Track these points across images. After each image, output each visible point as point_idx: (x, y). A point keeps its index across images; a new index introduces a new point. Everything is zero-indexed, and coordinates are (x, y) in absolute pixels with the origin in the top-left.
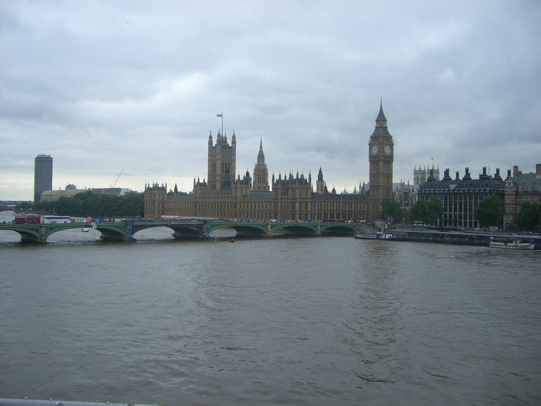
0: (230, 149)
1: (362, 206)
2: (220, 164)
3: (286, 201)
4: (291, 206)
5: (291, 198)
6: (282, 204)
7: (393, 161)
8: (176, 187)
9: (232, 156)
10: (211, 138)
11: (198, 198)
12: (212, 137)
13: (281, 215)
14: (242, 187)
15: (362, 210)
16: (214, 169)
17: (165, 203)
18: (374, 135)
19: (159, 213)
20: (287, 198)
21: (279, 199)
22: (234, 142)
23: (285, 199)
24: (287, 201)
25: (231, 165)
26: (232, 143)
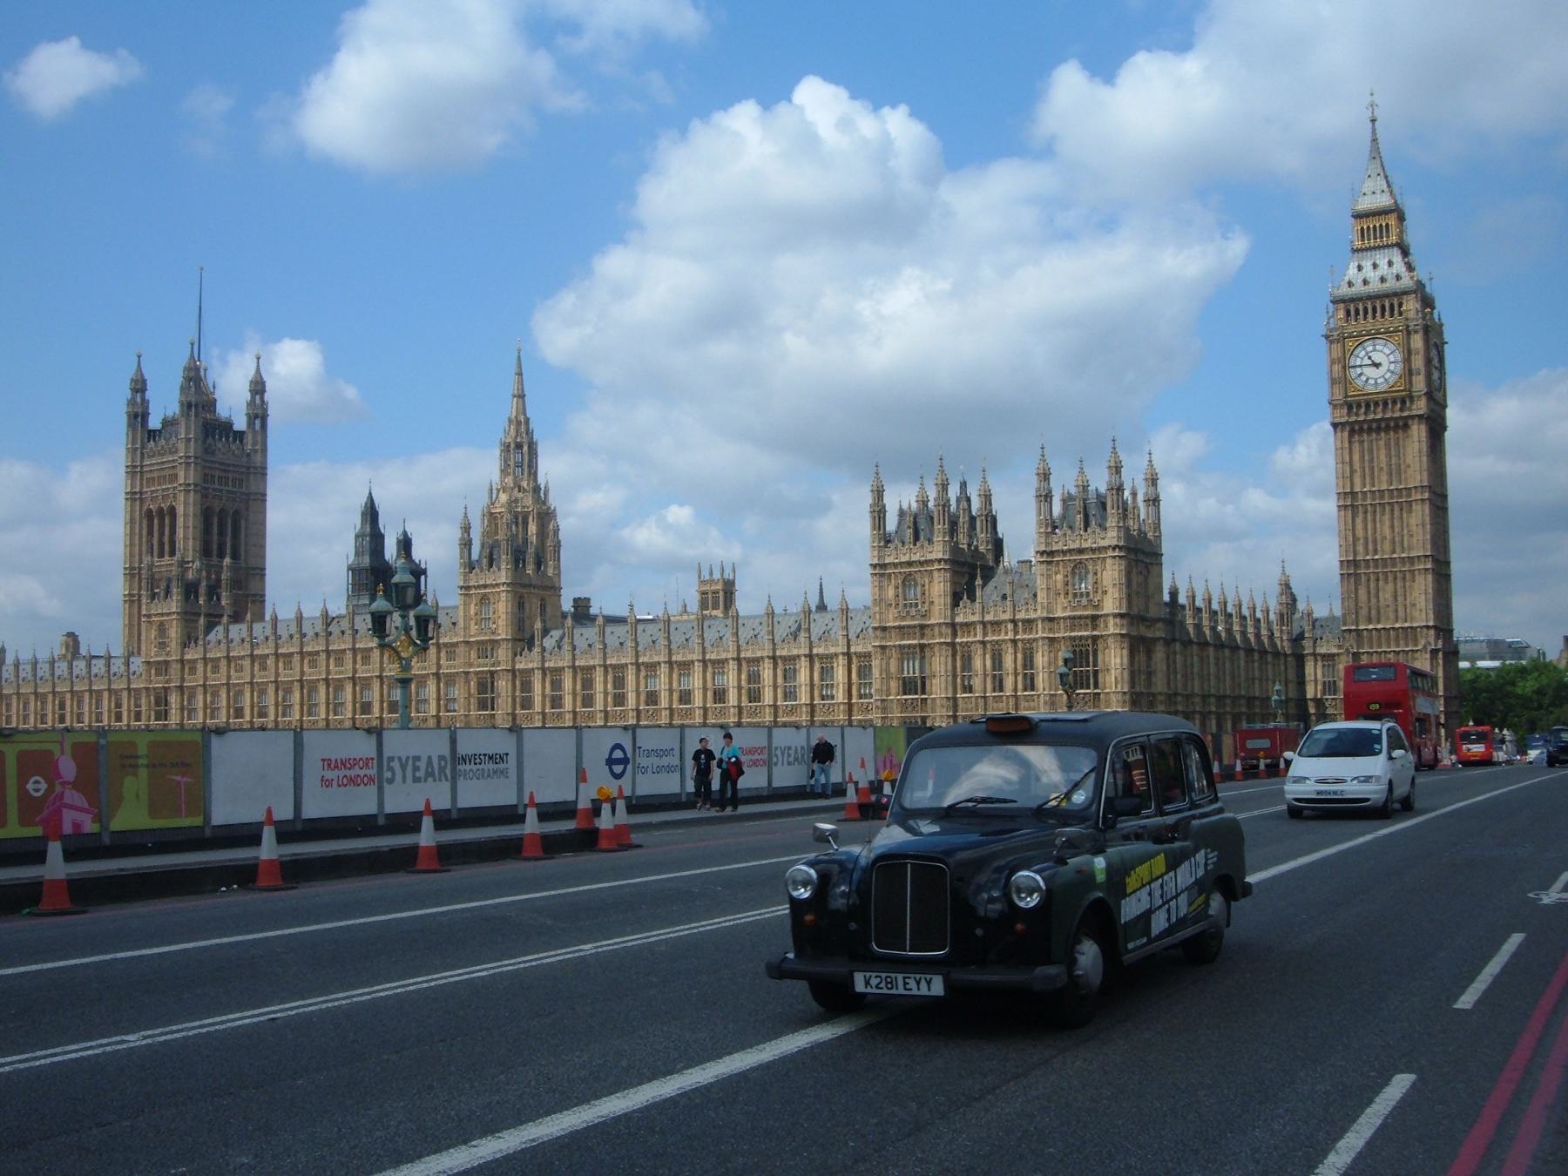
0: (241, 441)
1: (1292, 674)
3: (1010, 636)
5: (1059, 614)
7: (1444, 428)
9: (252, 477)
10: (139, 386)
11: (176, 667)
12: (144, 382)
14: (525, 586)
15: (1291, 695)
16: (162, 534)
18: (1359, 289)
22: (258, 414)
23: (997, 624)
24: (1014, 642)
25: (246, 520)
26: (252, 418)
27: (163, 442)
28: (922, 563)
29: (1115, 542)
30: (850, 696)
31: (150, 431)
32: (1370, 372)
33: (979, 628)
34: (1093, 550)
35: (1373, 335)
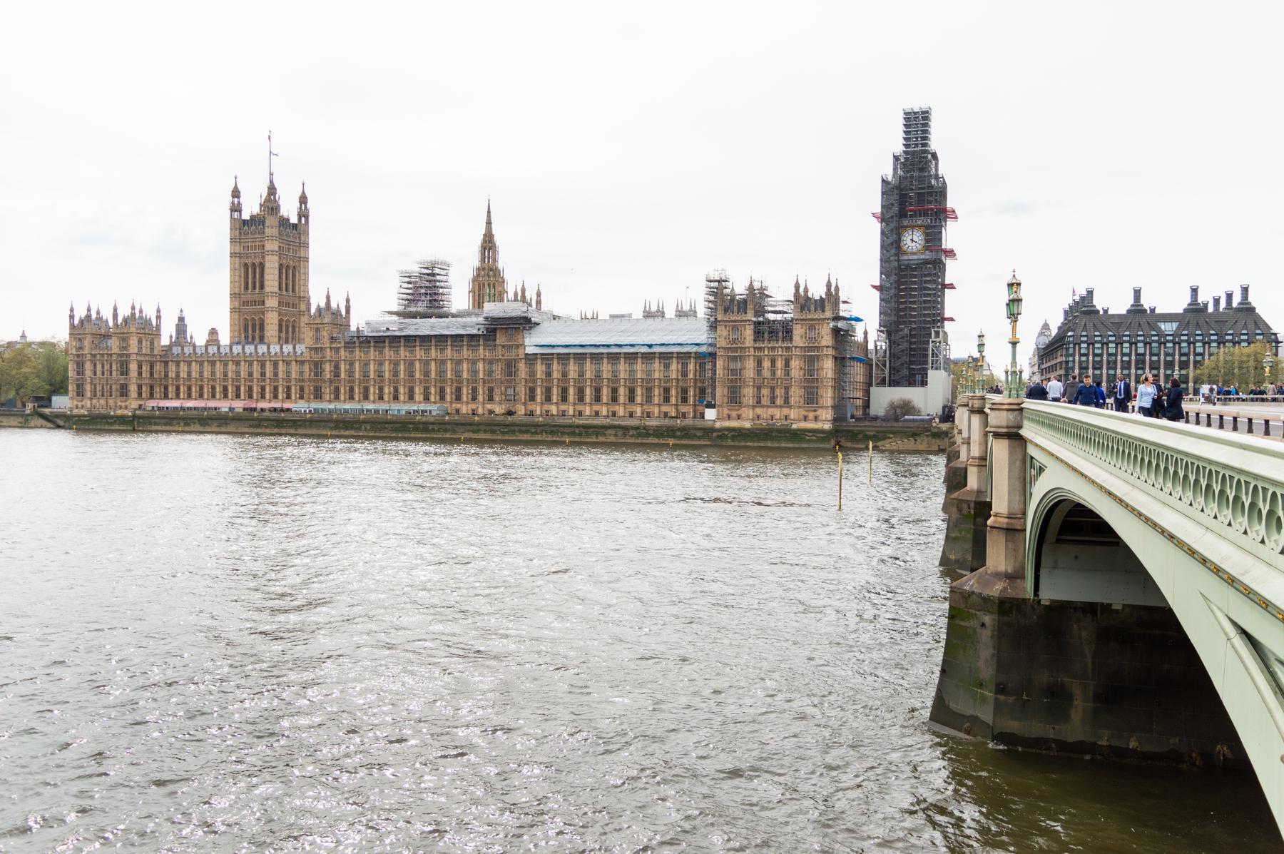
2: (277, 265)
3: (780, 353)
4: (801, 369)
6: (759, 363)
8: (181, 319)
10: (236, 193)
11: (328, 350)
13: (755, 393)
16: (254, 277)
17: (158, 364)
19: (140, 395)
20: (781, 347)
21: (752, 350)
22: (304, 214)
23: (773, 348)
25: (300, 272)
27: (254, 227)
28: (741, 321)
29: (827, 317)
30: (695, 376)
31: (244, 221)
32: (909, 242)
33: (766, 349)
34: (818, 320)
35: (913, 227)
